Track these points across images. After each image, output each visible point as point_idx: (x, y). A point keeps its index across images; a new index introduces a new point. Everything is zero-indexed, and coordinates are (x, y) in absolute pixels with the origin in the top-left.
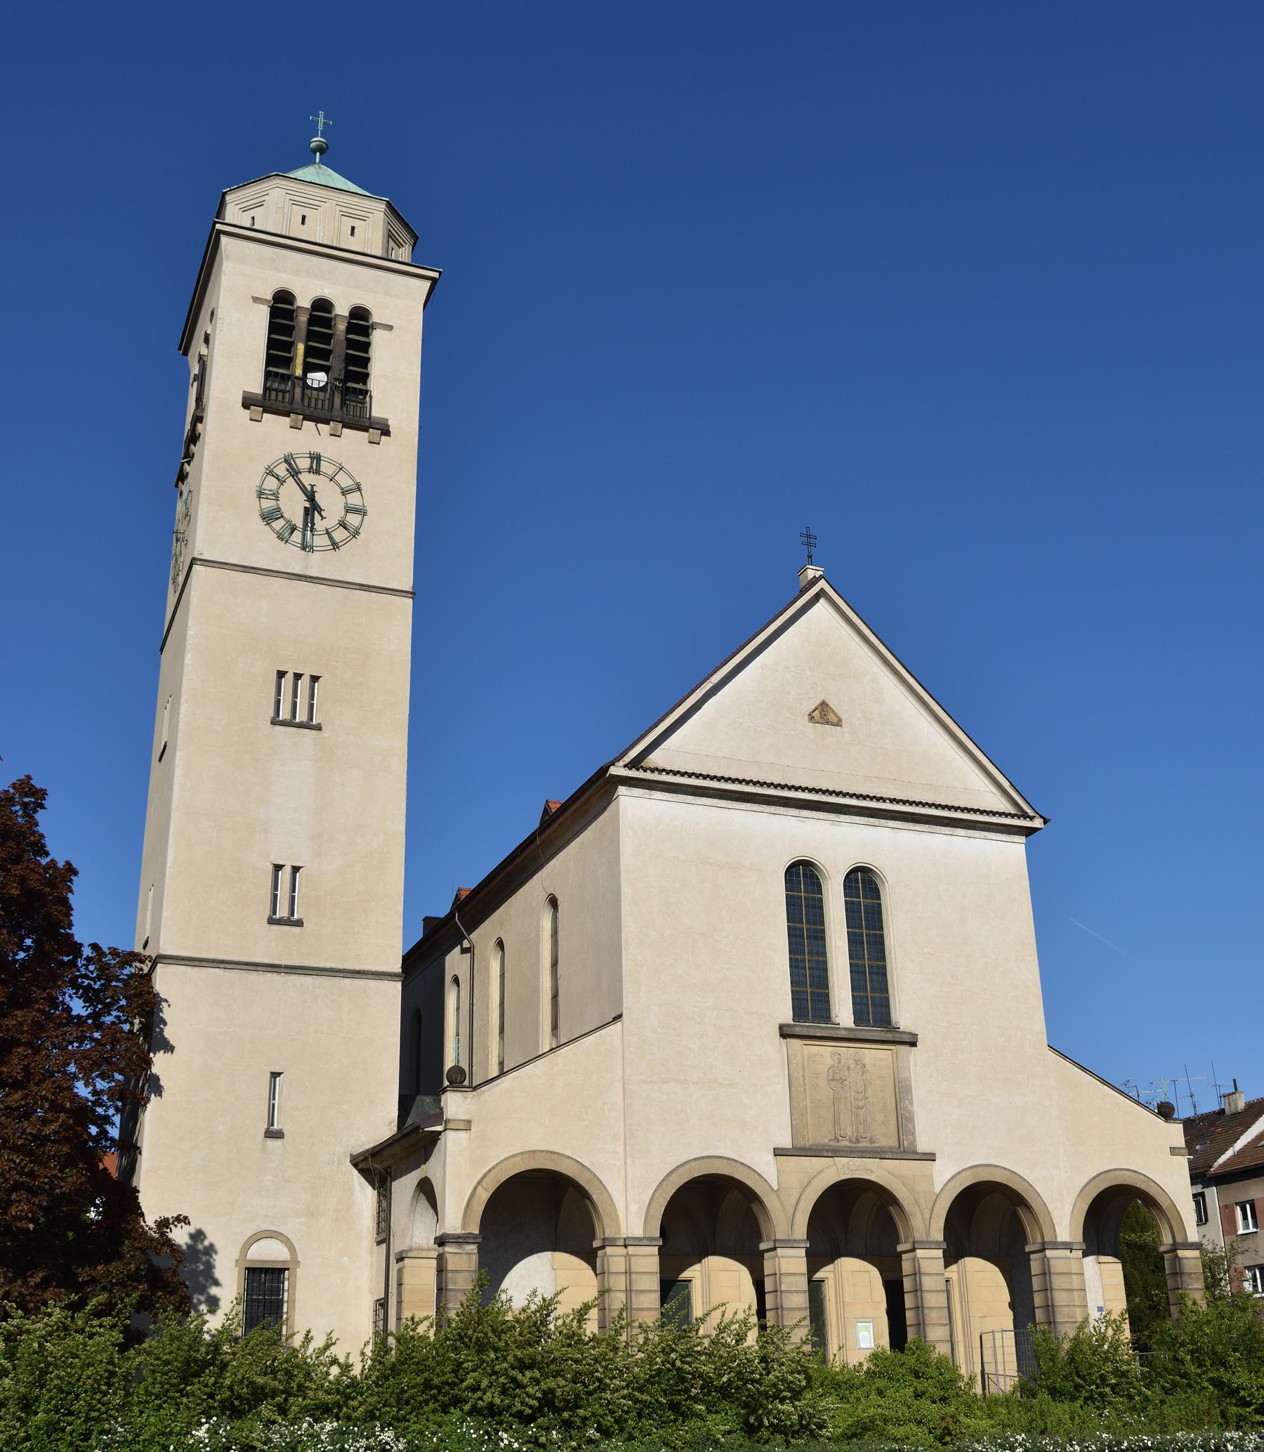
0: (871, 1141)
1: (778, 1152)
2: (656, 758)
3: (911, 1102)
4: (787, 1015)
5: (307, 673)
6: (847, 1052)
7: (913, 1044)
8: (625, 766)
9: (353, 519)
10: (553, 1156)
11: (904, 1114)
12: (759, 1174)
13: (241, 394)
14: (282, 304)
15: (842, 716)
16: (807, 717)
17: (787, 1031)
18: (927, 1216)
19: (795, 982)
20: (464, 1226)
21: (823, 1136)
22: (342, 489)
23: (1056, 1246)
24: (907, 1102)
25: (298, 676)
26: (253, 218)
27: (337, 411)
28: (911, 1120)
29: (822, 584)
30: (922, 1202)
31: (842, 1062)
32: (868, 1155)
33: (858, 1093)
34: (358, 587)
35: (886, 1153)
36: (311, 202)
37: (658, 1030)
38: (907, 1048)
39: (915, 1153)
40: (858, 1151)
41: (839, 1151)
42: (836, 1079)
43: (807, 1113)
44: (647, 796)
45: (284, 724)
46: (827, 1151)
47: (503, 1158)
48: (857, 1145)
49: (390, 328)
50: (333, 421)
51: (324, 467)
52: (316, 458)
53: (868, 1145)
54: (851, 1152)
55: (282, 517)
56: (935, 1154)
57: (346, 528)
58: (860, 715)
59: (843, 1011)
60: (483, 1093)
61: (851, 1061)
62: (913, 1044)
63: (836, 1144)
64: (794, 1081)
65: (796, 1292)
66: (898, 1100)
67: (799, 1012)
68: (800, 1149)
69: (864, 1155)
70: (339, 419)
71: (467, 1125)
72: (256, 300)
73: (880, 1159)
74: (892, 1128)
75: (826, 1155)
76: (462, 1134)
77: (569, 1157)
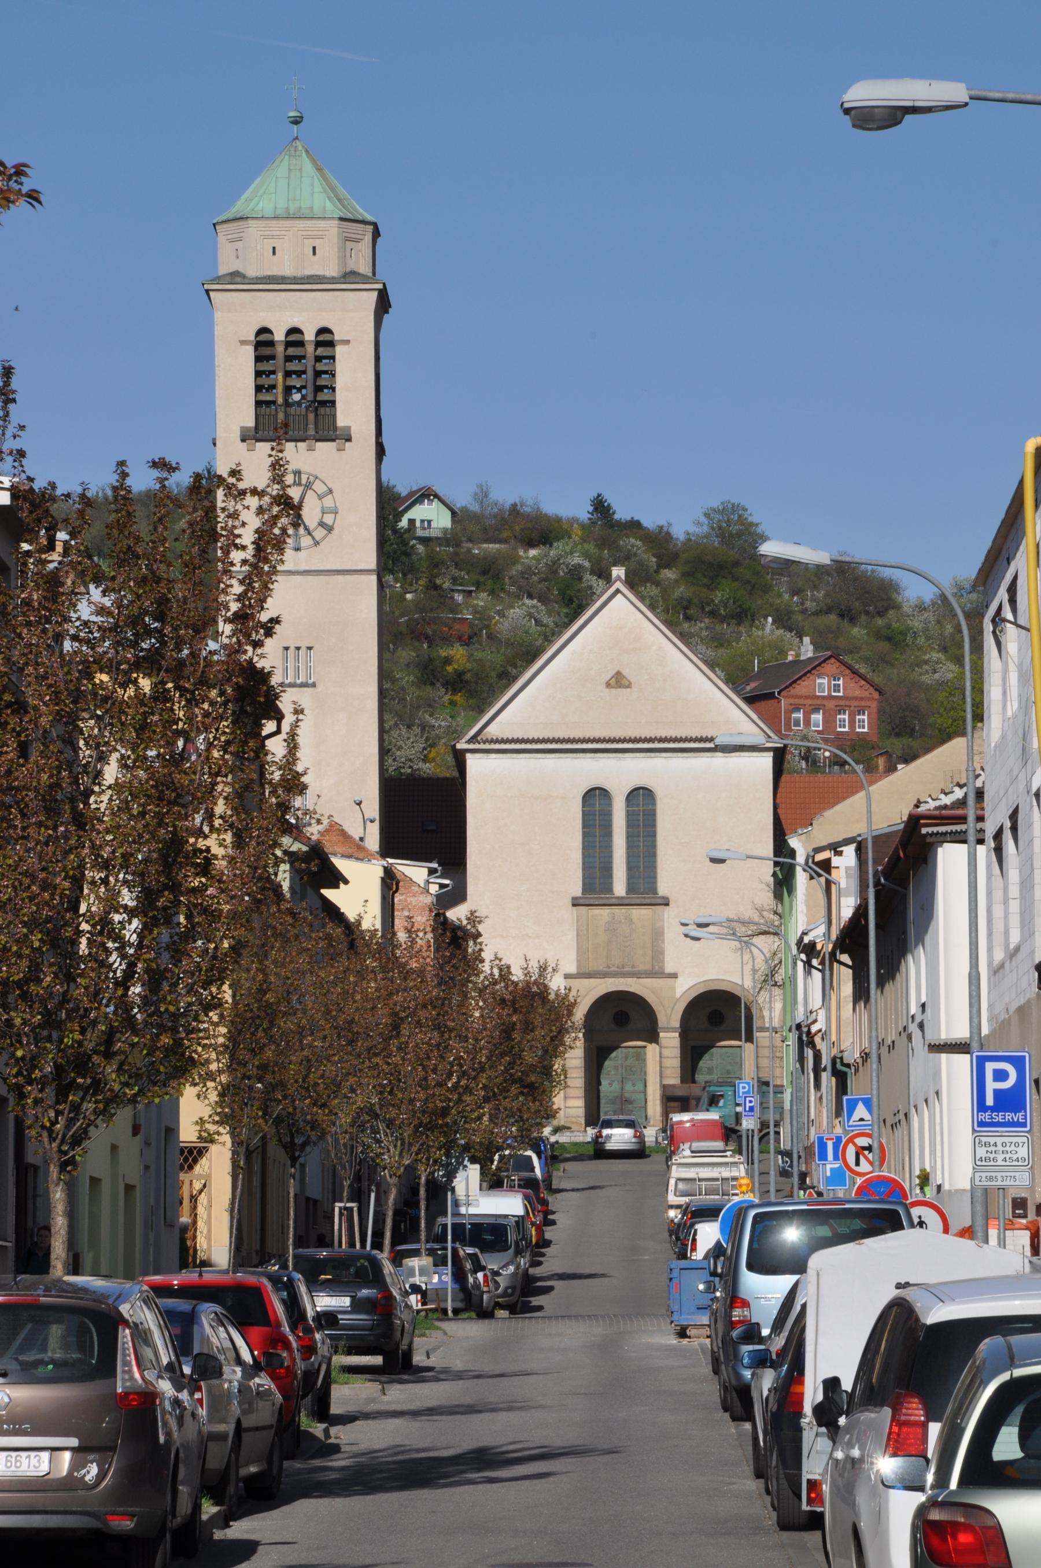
0: (633, 966)
2: (493, 730)
3: (663, 941)
4: (577, 890)
5: (304, 645)
7: (667, 904)
14: (263, 341)
15: (632, 680)
17: (576, 902)
18: (669, 1012)
21: (601, 967)
23: (762, 1029)
27: (311, 432)
28: (662, 953)
38: (663, 907)
39: (663, 973)
42: (611, 929)
49: (347, 342)
59: (620, 888)
67: (588, 886)
72: (243, 343)
74: (648, 959)
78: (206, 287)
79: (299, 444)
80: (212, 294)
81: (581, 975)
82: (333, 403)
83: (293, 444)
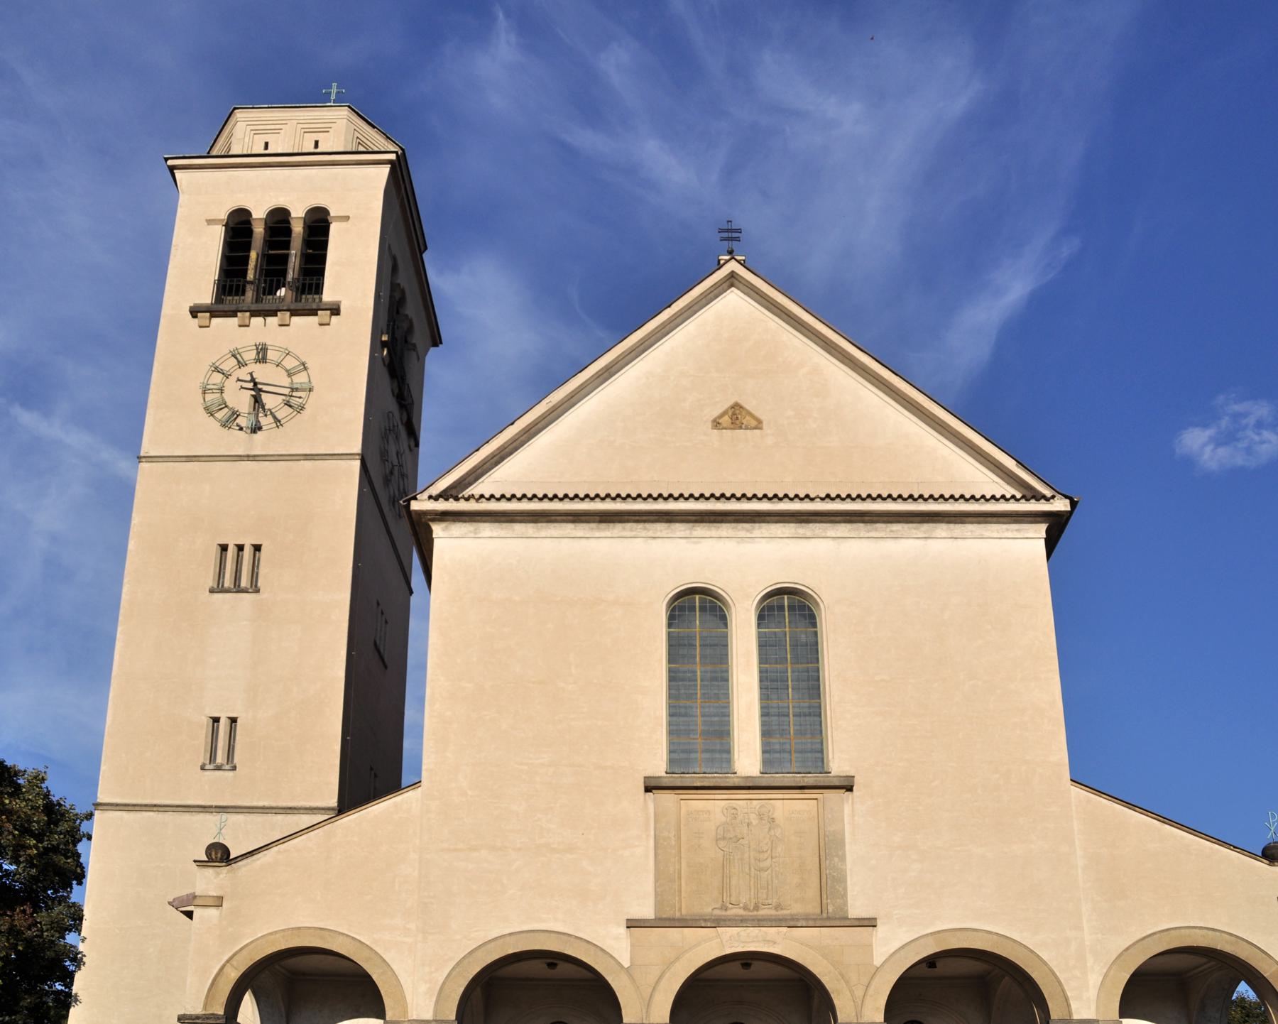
1: (632, 924)
3: (843, 859)
4: (658, 766)
6: (747, 805)
7: (850, 789)
10: (323, 932)
11: (830, 874)
12: (602, 950)
18: (859, 993)
19: (673, 732)
20: (205, 1007)
22: (287, 371)
24: (836, 859)
28: (842, 880)
31: (740, 817)
32: (769, 924)
34: (302, 458)
35: (798, 920)
37: (470, 793)
39: (846, 918)
40: (753, 920)
41: (724, 920)
43: (680, 878)
47: (259, 935)
48: (755, 913)
50: (280, 311)
53: (773, 912)
55: (226, 406)
56: (875, 919)
57: (290, 406)
60: (239, 868)
61: (753, 816)
62: (850, 789)
63: (723, 913)
64: (661, 841)
66: (823, 858)
68: (661, 919)
69: (762, 924)
70: (285, 308)
71: (218, 902)
73: (788, 927)
74: (812, 892)
75: (703, 925)
76: (213, 912)
77: (344, 934)
79: (269, 319)
83: (260, 319)
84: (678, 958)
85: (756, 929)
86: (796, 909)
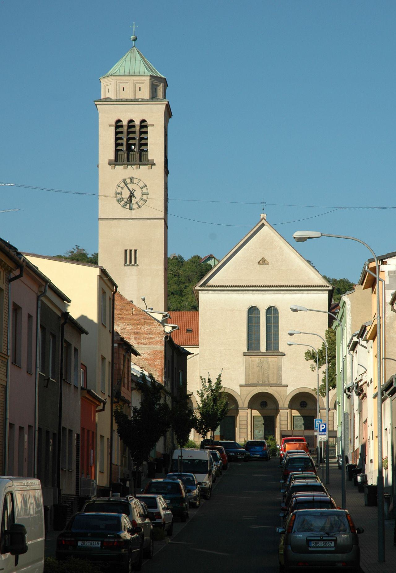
1: (241, 386)
2: (211, 282)
4: (246, 350)
6: (263, 358)
7: (284, 355)
8: (199, 287)
9: (145, 197)
13: (108, 160)
14: (118, 124)
15: (269, 261)
16: (257, 263)
17: (245, 354)
18: (284, 401)
21: (253, 381)
25: (131, 251)
26: (109, 89)
28: (281, 376)
29: (263, 221)
30: (283, 398)
33: (266, 369)
35: (272, 385)
36: (125, 82)
37: (209, 356)
39: (282, 385)
42: (260, 366)
44: (207, 293)
45: (128, 265)
46: (254, 385)
51: (136, 181)
52: (132, 179)
53: (267, 383)
54: (262, 385)
58: (275, 260)
59: (263, 348)
63: (258, 383)
65: (244, 420)
68: (247, 385)
72: (110, 125)
74: (275, 378)
78: (95, 103)
80: (97, 105)
81: (246, 385)
82: (147, 151)
84: (249, 393)
85: (264, 387)
86: (272, 382)
